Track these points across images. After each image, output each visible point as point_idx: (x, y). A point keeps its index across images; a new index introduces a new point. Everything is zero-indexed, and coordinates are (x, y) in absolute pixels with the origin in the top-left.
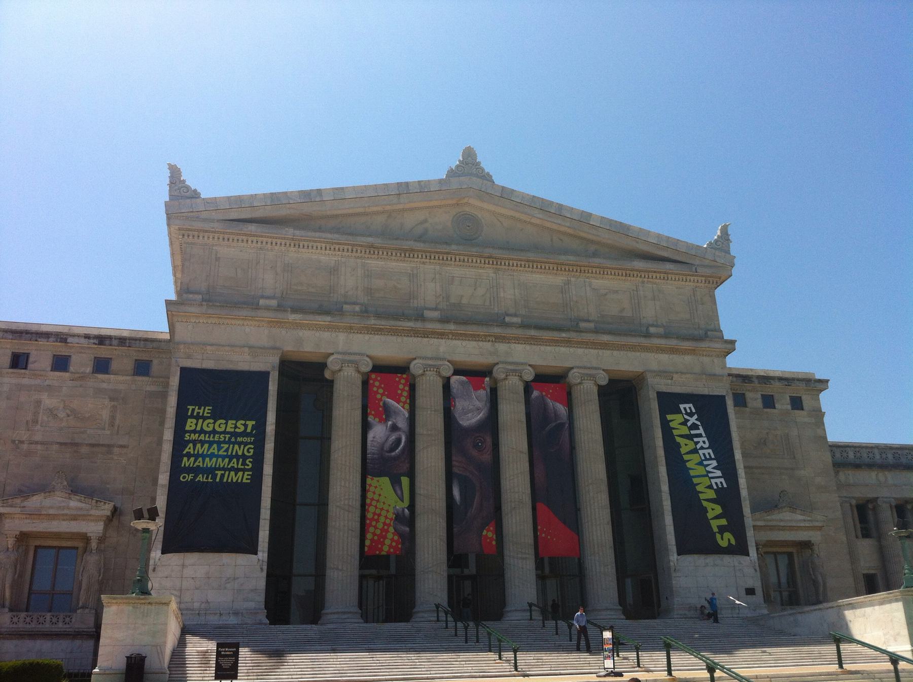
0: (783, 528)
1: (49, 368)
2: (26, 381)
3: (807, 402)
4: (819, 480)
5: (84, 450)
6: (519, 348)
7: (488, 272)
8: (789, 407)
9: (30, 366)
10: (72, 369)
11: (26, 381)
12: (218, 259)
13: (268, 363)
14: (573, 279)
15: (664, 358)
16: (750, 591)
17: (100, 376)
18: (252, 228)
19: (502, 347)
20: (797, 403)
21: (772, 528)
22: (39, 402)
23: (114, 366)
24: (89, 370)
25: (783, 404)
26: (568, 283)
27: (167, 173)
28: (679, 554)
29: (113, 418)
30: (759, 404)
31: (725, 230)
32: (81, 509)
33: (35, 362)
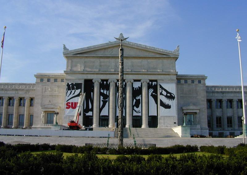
0: (190, 110)
2: (43, 84)
3: (202, 81)
4: (202, 99)
6: (130, 76)
8: (198, 83)
10: (51, 81)
14: (143, 60)
16: (175, 123)
17: (56, 82)
18: (78, 55)
20: (200, 82)
21: (188, 110)
25: (196, 82)
27: (63, 46)
31: (178, 46)
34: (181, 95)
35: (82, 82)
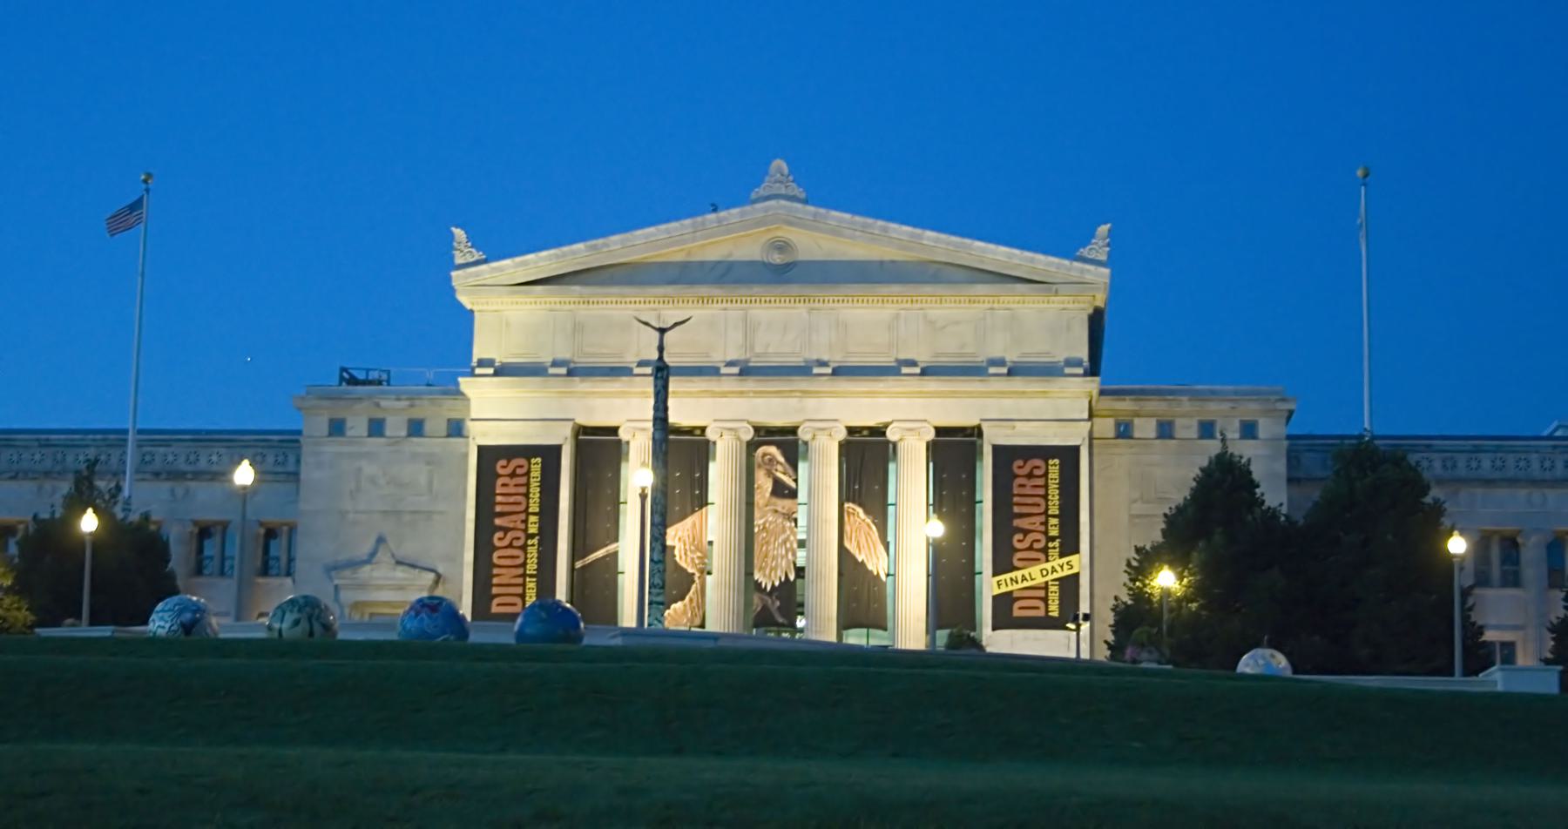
1: (366, 434)
5: (407, 518)
6: (831, 401)
7: (799, 311)
9: (349, 433)
10: (388, 433)
11: (346, 449)
12: (508, 324)
13: (561, 436)
15: (1008, 402)
17: (415, 440)
19: (811, 402)
22: (359, 470)
23: (428, 427)
24: (404, 433)
26: (897, 316)
28: (994, 628)
29: (430, 483)
30: (1193, 433)
32: (405, 579)
33: (352, 428)
34: (1138, 508)
35: (561, 436)
